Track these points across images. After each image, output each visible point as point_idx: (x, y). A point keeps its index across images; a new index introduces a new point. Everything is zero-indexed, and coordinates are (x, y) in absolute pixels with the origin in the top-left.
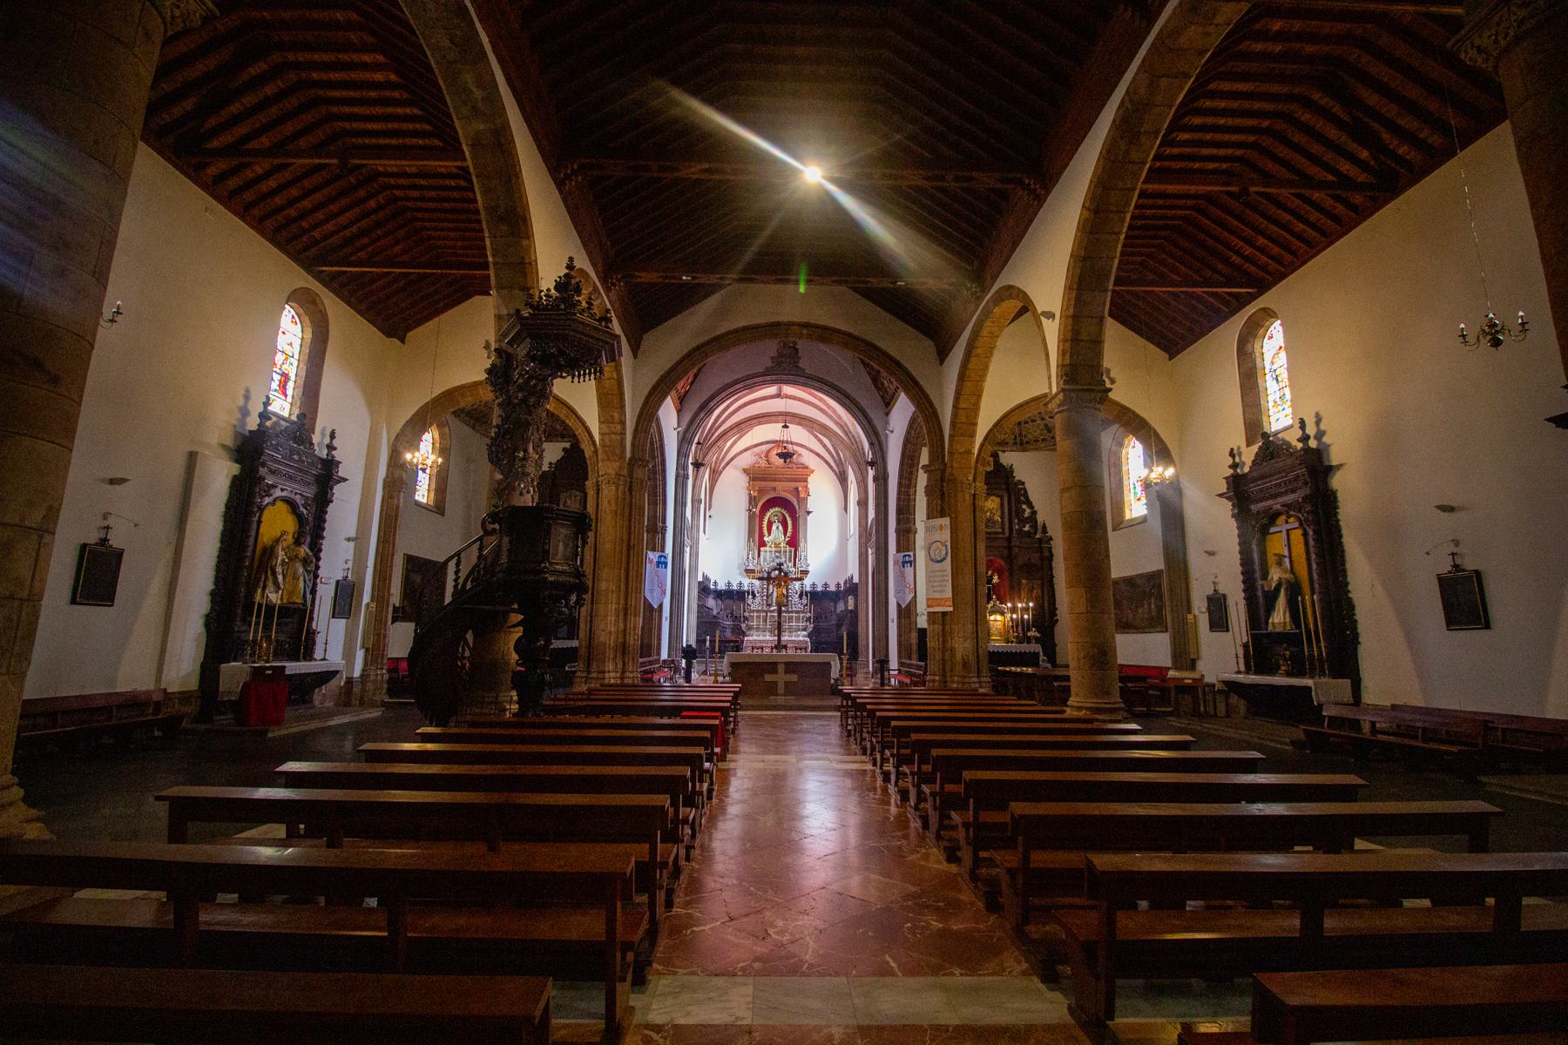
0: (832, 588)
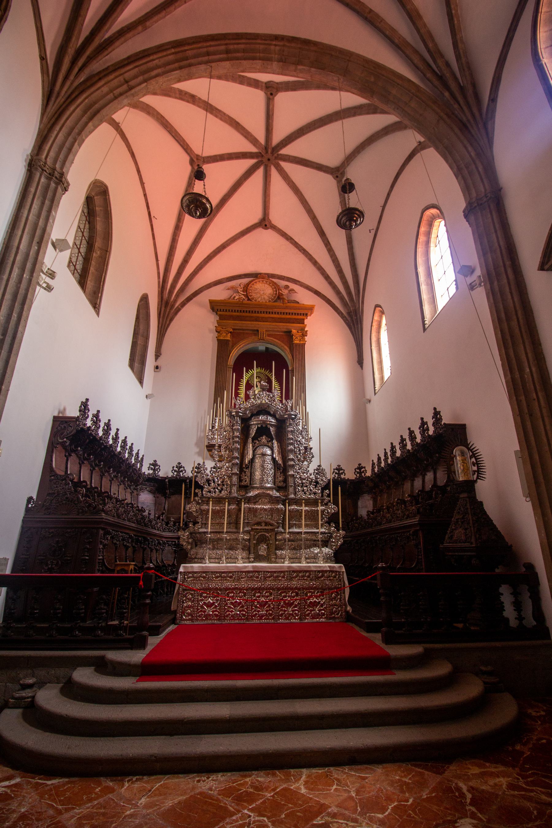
0: (350, 475)
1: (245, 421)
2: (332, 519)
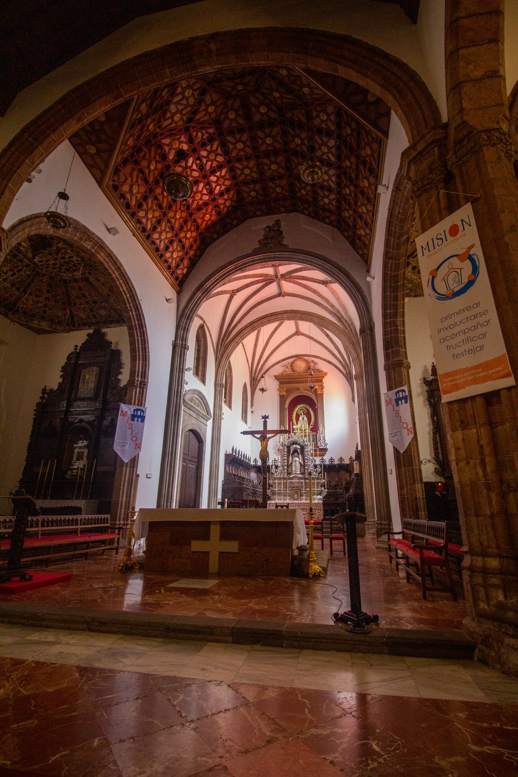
1: (288, 447)
2: (323, 485)
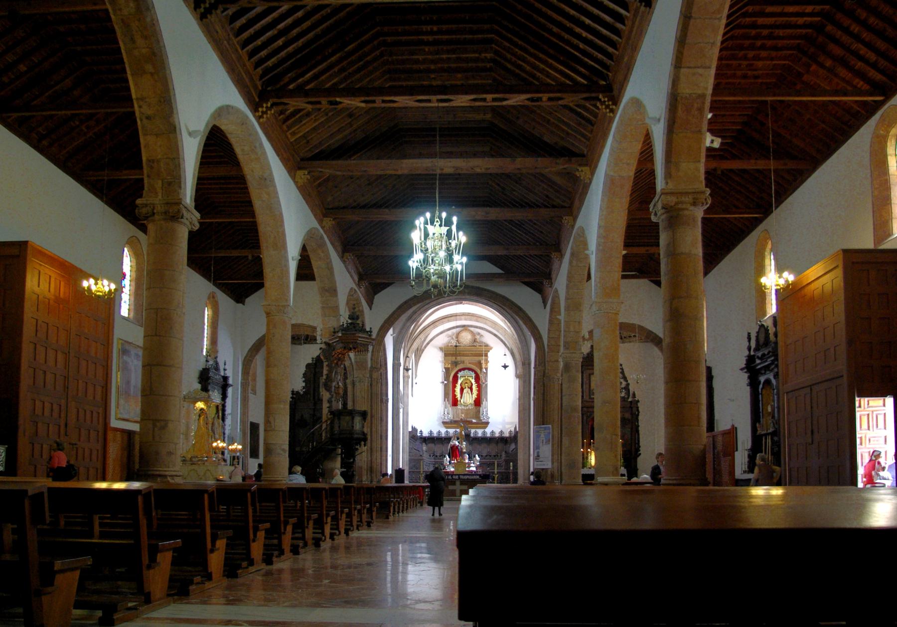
0: (507, 435)
